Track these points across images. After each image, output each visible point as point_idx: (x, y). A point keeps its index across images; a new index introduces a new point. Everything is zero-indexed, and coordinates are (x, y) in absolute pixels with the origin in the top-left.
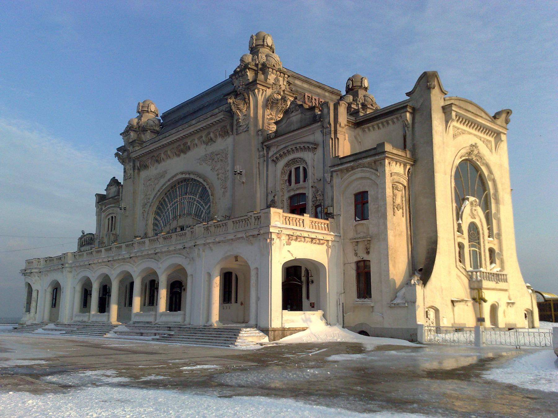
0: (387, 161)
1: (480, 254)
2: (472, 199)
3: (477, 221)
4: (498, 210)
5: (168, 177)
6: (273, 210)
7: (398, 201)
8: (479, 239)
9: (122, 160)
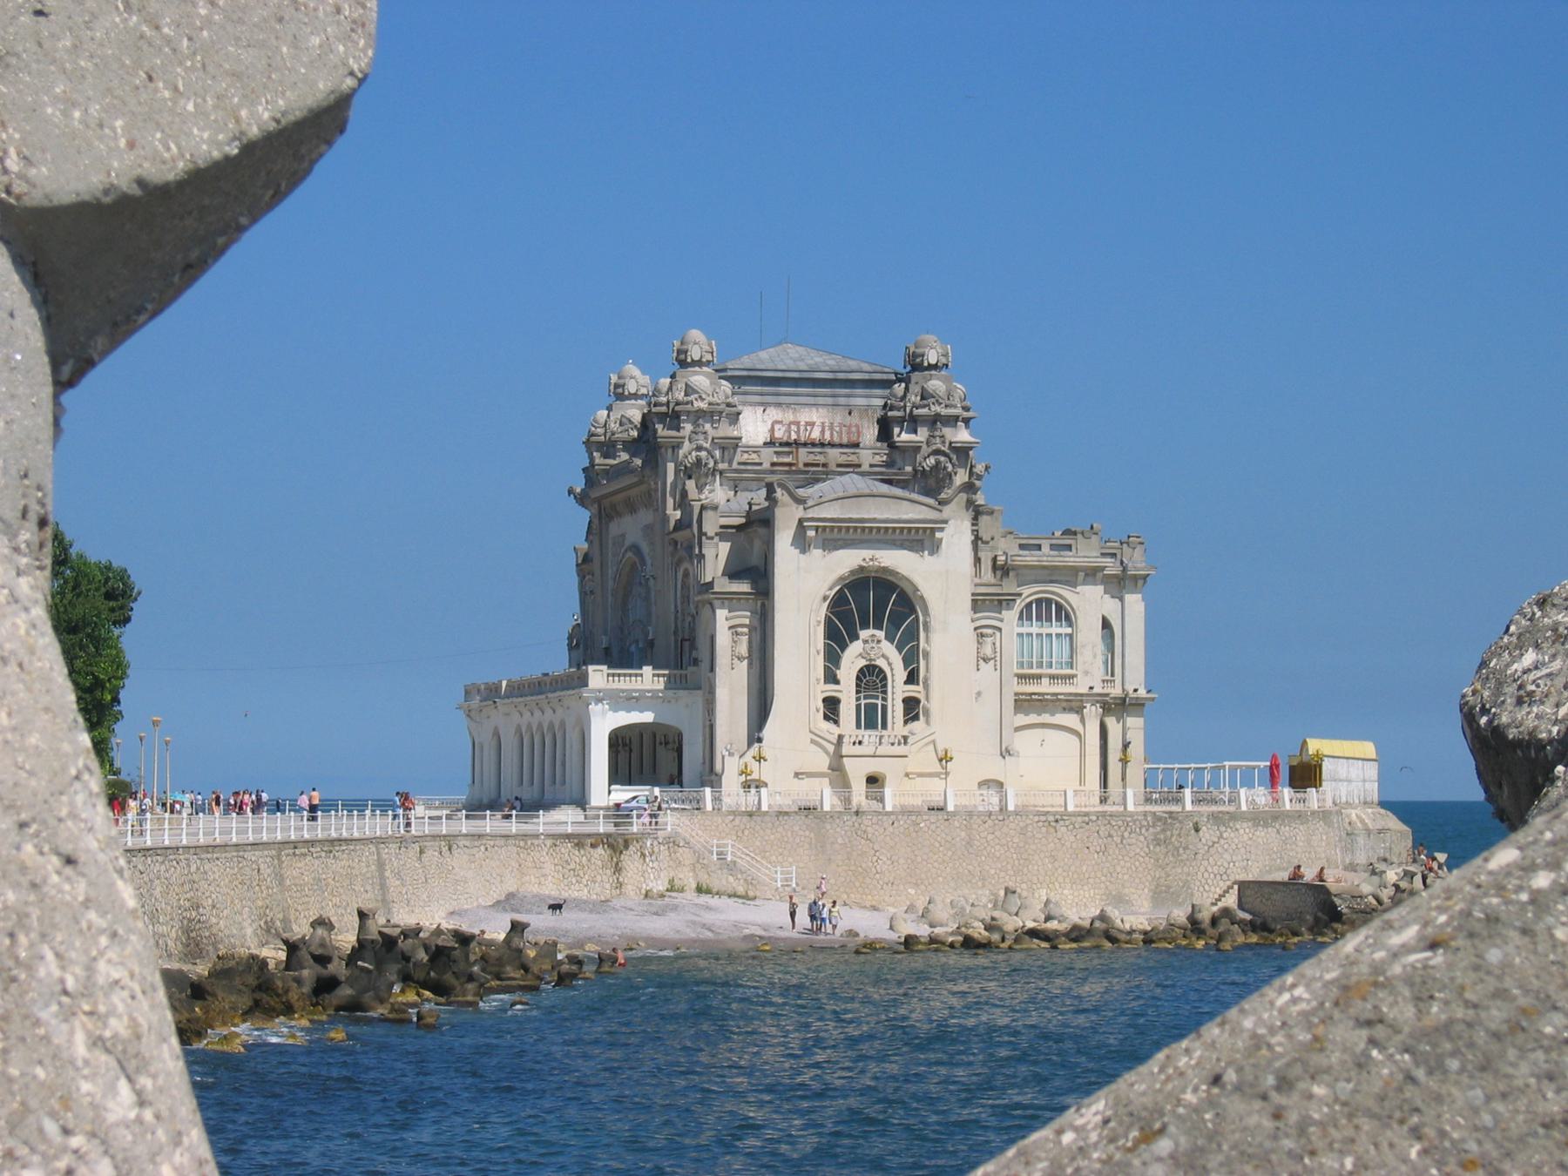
0: (716, 603)
1: (884, 708)
2: (864, 634)
3: (881, 663)
5: (627, 543)
6: (591, 668)
7: (743, 649)
8: (885, 686)
9: (582, 499)
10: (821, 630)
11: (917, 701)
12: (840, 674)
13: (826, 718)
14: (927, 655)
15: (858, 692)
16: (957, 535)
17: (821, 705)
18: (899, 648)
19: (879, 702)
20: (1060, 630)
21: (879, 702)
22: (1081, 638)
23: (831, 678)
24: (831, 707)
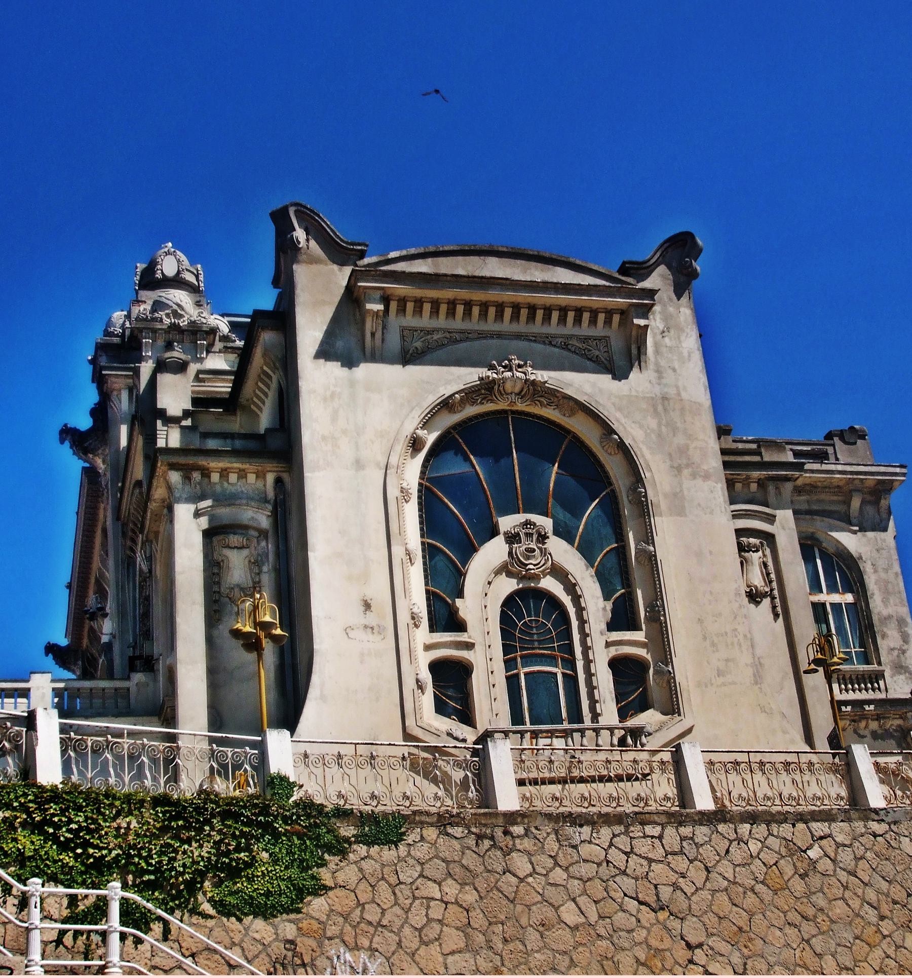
1: (571, 681)
2: (507, 523)
3: (549, 584)
4: (647, 536)
10: (410, 516)
11: (639, 665)
12: (466, 607)
13: (441, 708)
14: (651, 561)
15: (507, 649)
16: (674, 335)
17: (426, 676)
18: (587, 551)
19: (558, 671)
20: (836, 598)
21: (558, 671)
22: (878, 605)
23: (444, 618)
24: (452, 682)
